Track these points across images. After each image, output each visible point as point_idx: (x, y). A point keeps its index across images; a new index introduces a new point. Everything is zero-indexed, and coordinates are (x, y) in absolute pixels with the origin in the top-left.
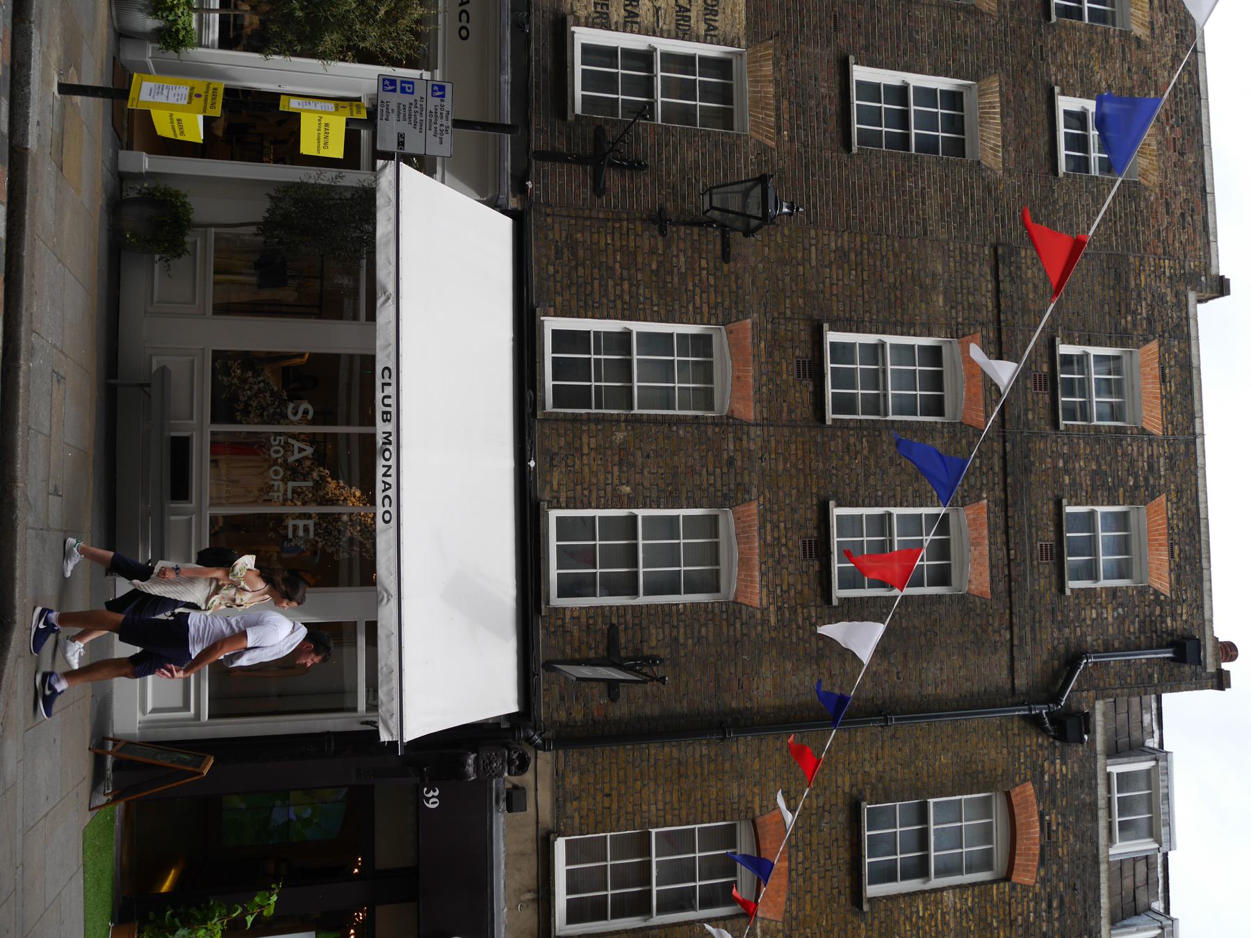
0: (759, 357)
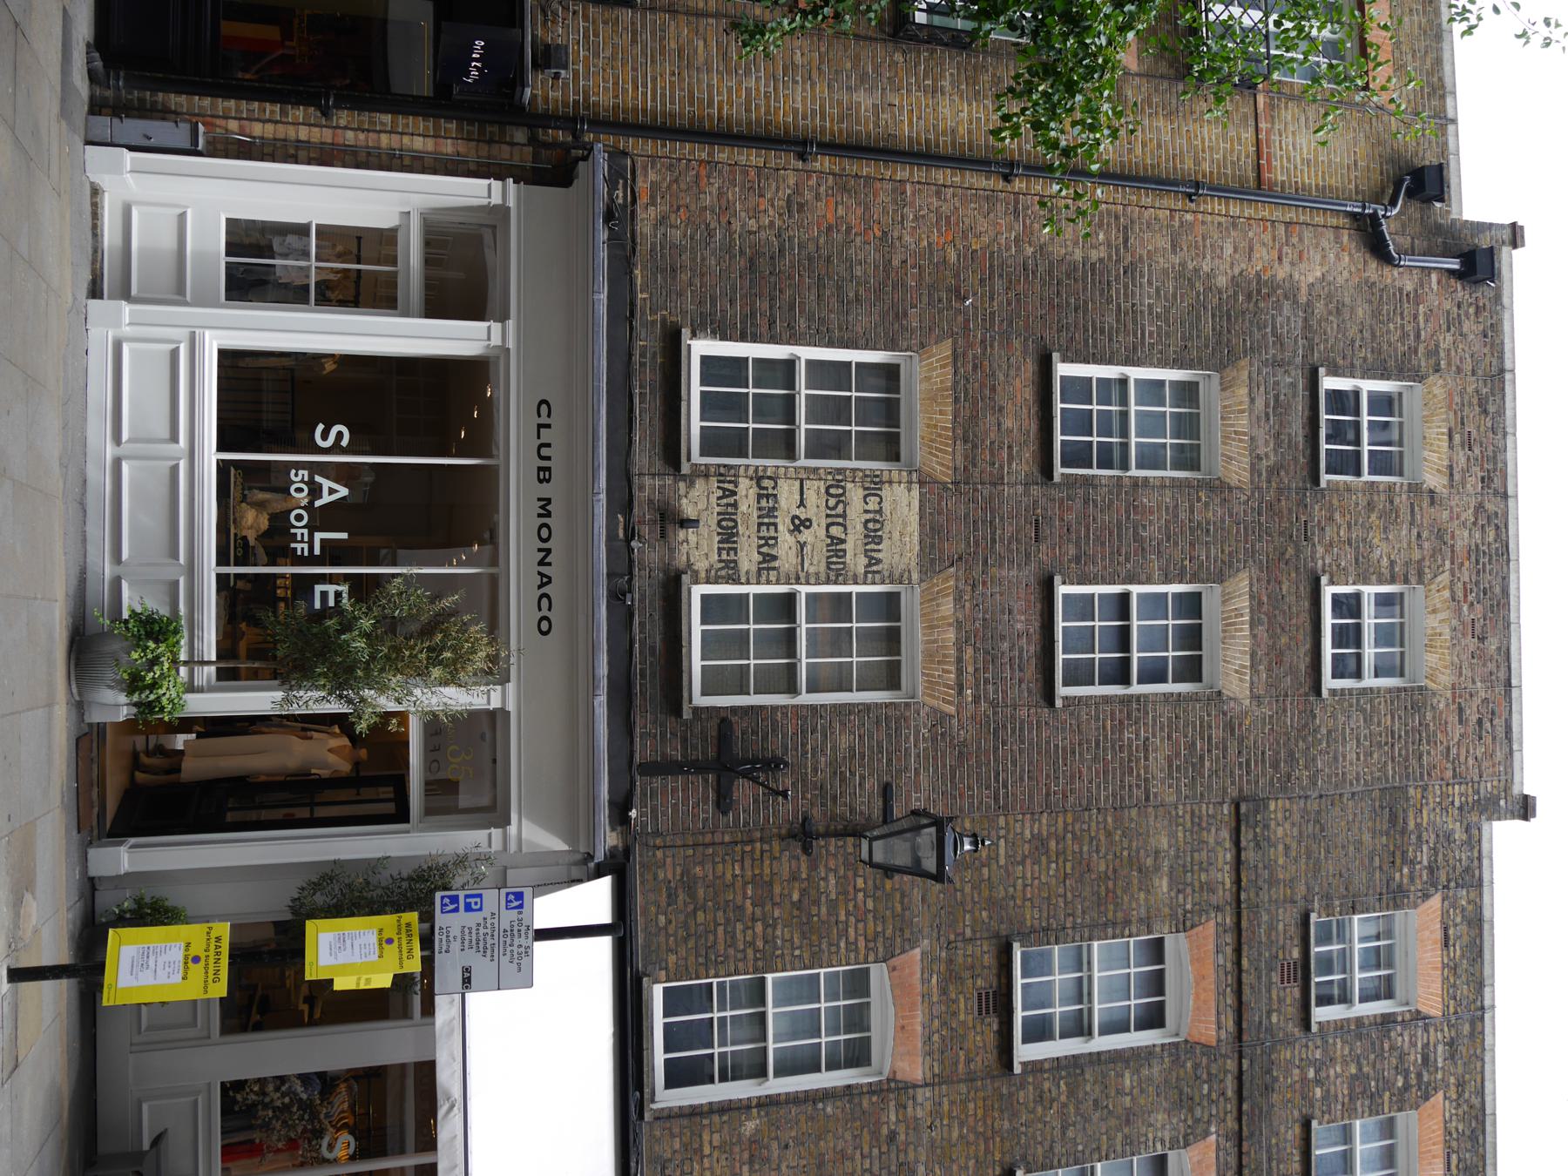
0: (930, 995)
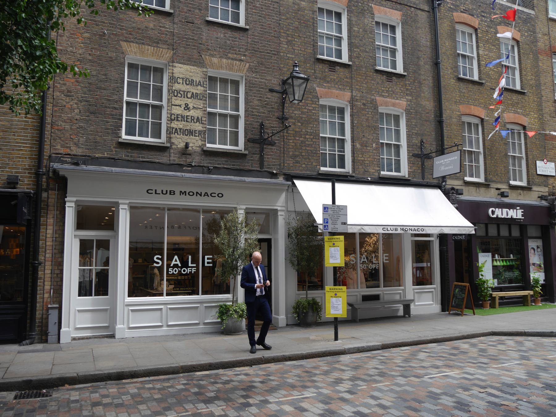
0: (329, 87)
